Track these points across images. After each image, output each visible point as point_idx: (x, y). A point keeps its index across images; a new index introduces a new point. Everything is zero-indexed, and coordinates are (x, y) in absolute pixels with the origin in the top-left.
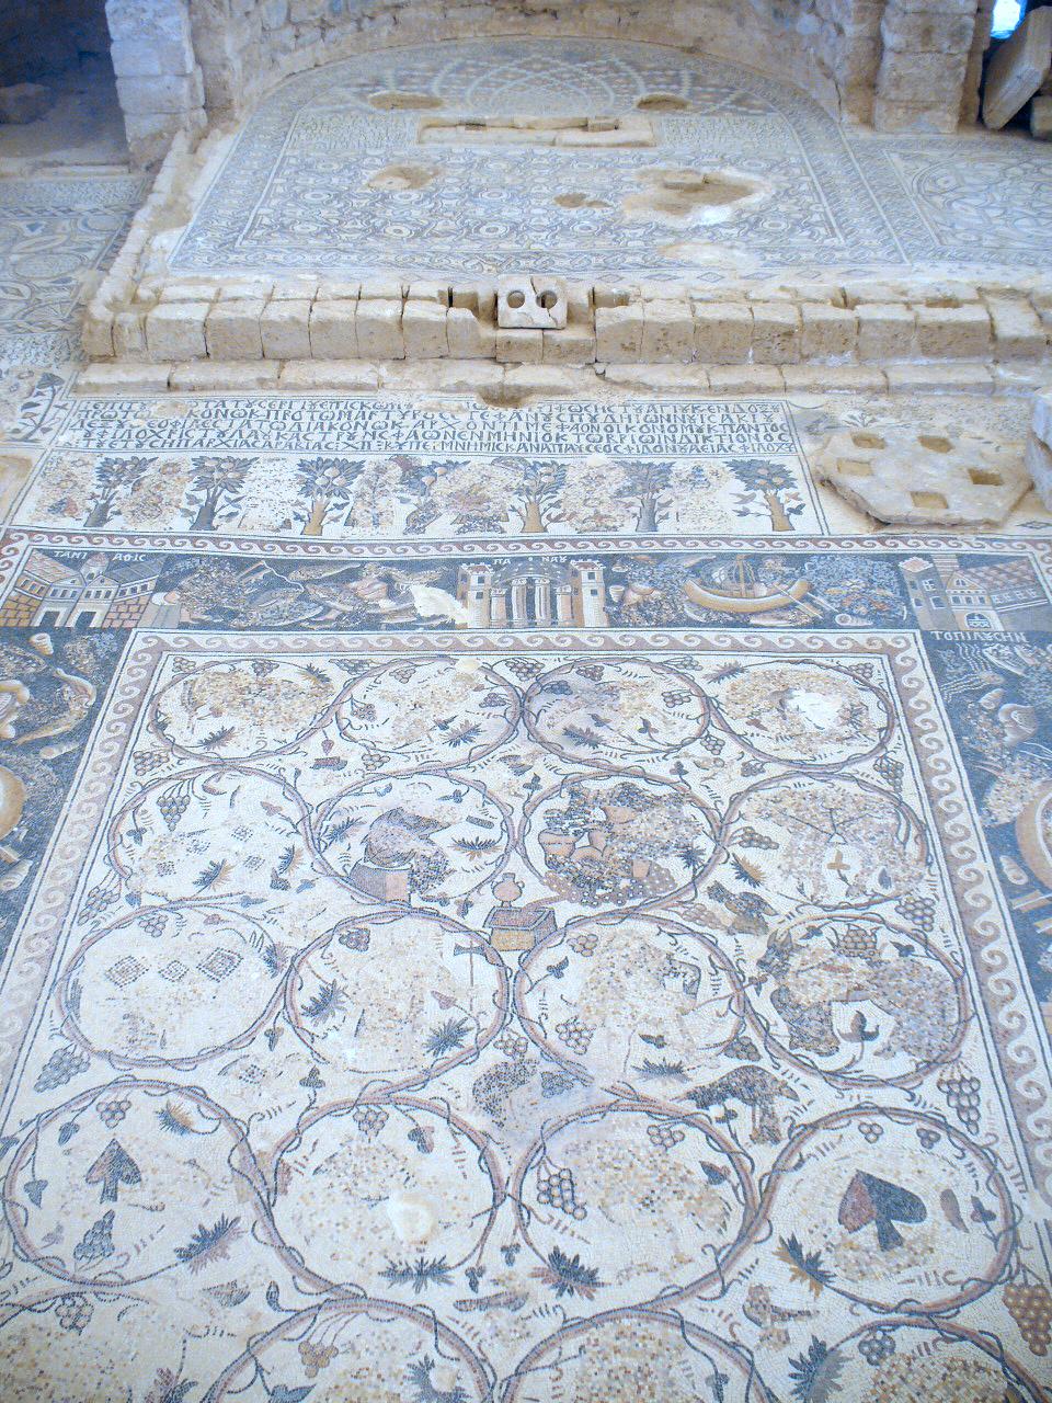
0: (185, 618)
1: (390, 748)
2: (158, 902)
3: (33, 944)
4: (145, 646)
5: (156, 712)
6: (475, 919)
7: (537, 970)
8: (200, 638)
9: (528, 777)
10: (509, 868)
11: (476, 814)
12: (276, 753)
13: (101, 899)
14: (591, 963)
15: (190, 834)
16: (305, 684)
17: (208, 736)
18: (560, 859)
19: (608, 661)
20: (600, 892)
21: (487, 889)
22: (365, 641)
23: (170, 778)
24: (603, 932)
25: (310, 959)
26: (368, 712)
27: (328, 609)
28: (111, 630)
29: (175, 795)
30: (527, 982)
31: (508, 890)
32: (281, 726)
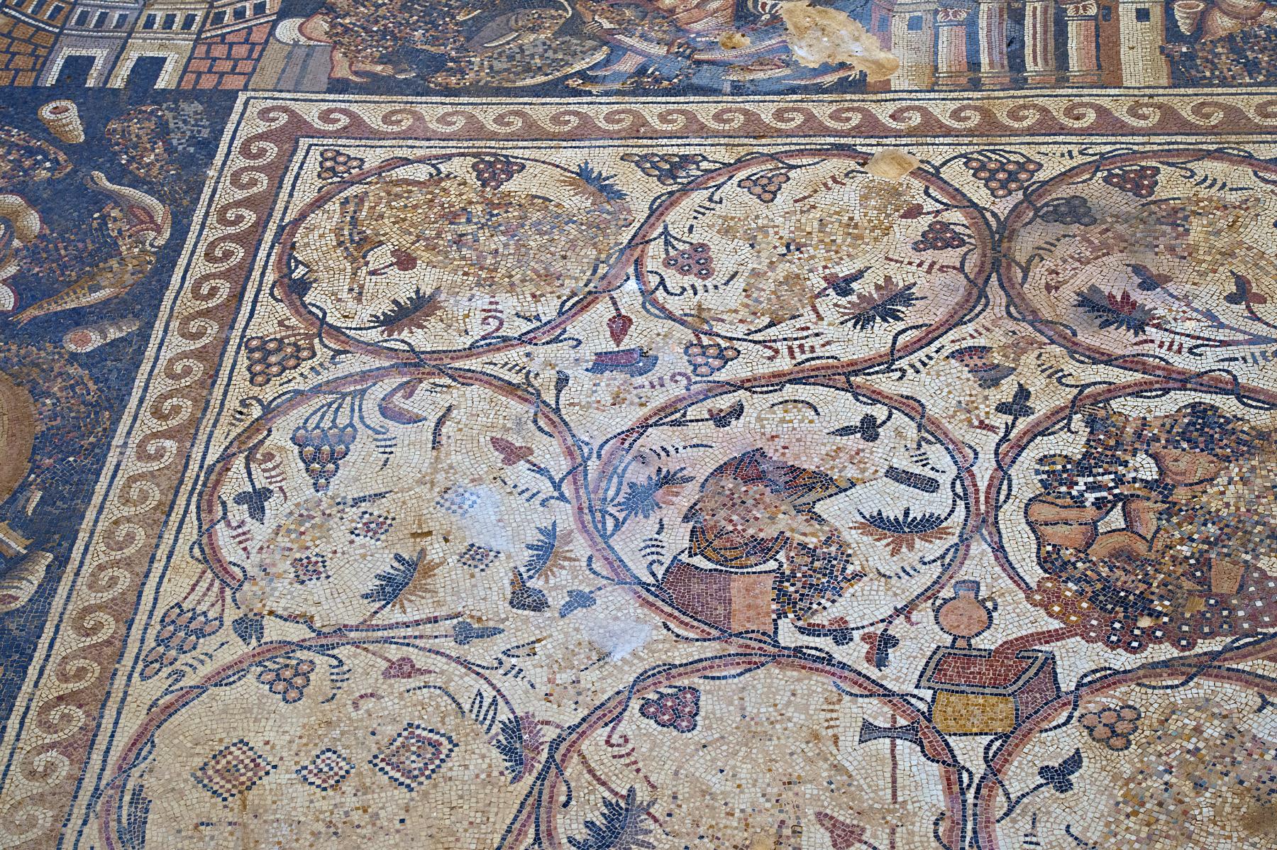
0: (342, 71)
1: (740, 331)
2: (296, 632)
3: (54, 716)
4: (262, 127)
5: (287, 260)
6: (902, 671)
7: (1020, 775)
8: (371, 112)
9: (1006, 391)
10: (969, 571)
11: (903, 462)
12: (522, 340)
13: (185, 628)
14: (1126, 762)
15: (356, 502)
16: (575, 202)
17: (386, 307)
18: (1068, 554)
19: (1167, 156)
20: (1145, 622)
21: (924, 615)
22: (691, 118)
23: (317, 390)
24: (1150, 701)
25: (585, 746)
26: (697, 261)
27: (617, 51)
28: (195, 95)
29: (326, 424)
30: (1001, 798)
31: (965, 616)
32: (529, 288)
